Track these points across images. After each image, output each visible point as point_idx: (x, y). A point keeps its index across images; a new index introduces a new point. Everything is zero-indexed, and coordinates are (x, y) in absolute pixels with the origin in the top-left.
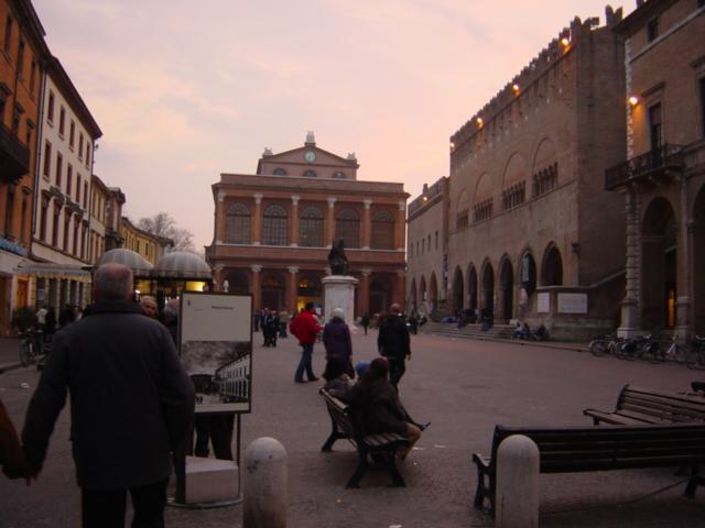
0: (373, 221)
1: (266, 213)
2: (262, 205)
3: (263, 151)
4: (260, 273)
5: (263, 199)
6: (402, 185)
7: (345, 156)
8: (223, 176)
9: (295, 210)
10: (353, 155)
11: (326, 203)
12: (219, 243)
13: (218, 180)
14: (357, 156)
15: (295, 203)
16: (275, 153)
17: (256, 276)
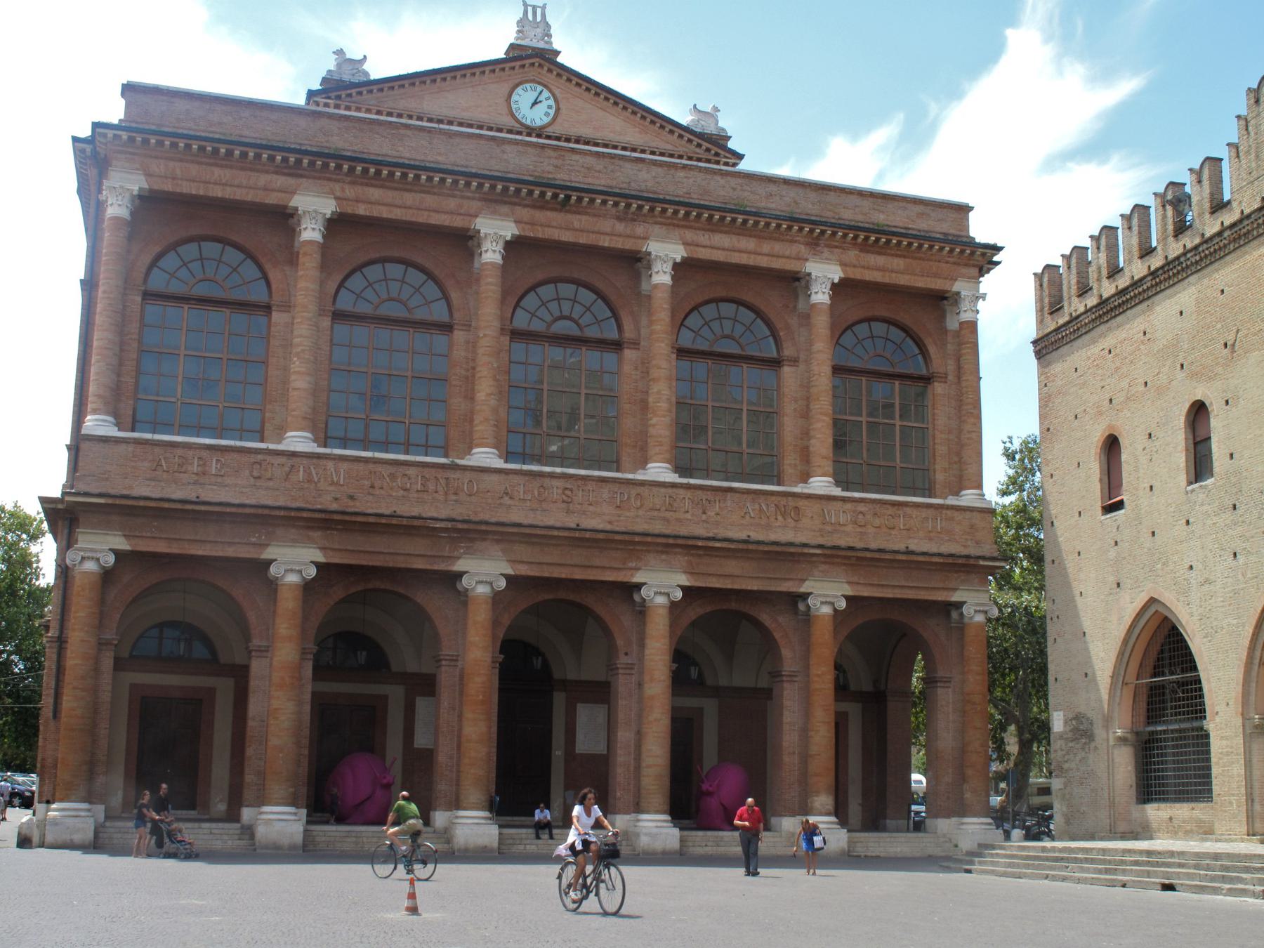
0: (837, 370)
1: (346, 302)
2: (325, 248)
3: (330, 64)
4: (308, 587)
5: (337, 225)
6: (964, 210)
7: (684, 118)
8: (130, 90)
9: (490, 287)
10: (712, 115)
11: (635, 262)
12: (96, 424)
13: (115, 111)
14: (726, 123)
15: (491, 254)
16: (377, 70)
17: (288, 603)
